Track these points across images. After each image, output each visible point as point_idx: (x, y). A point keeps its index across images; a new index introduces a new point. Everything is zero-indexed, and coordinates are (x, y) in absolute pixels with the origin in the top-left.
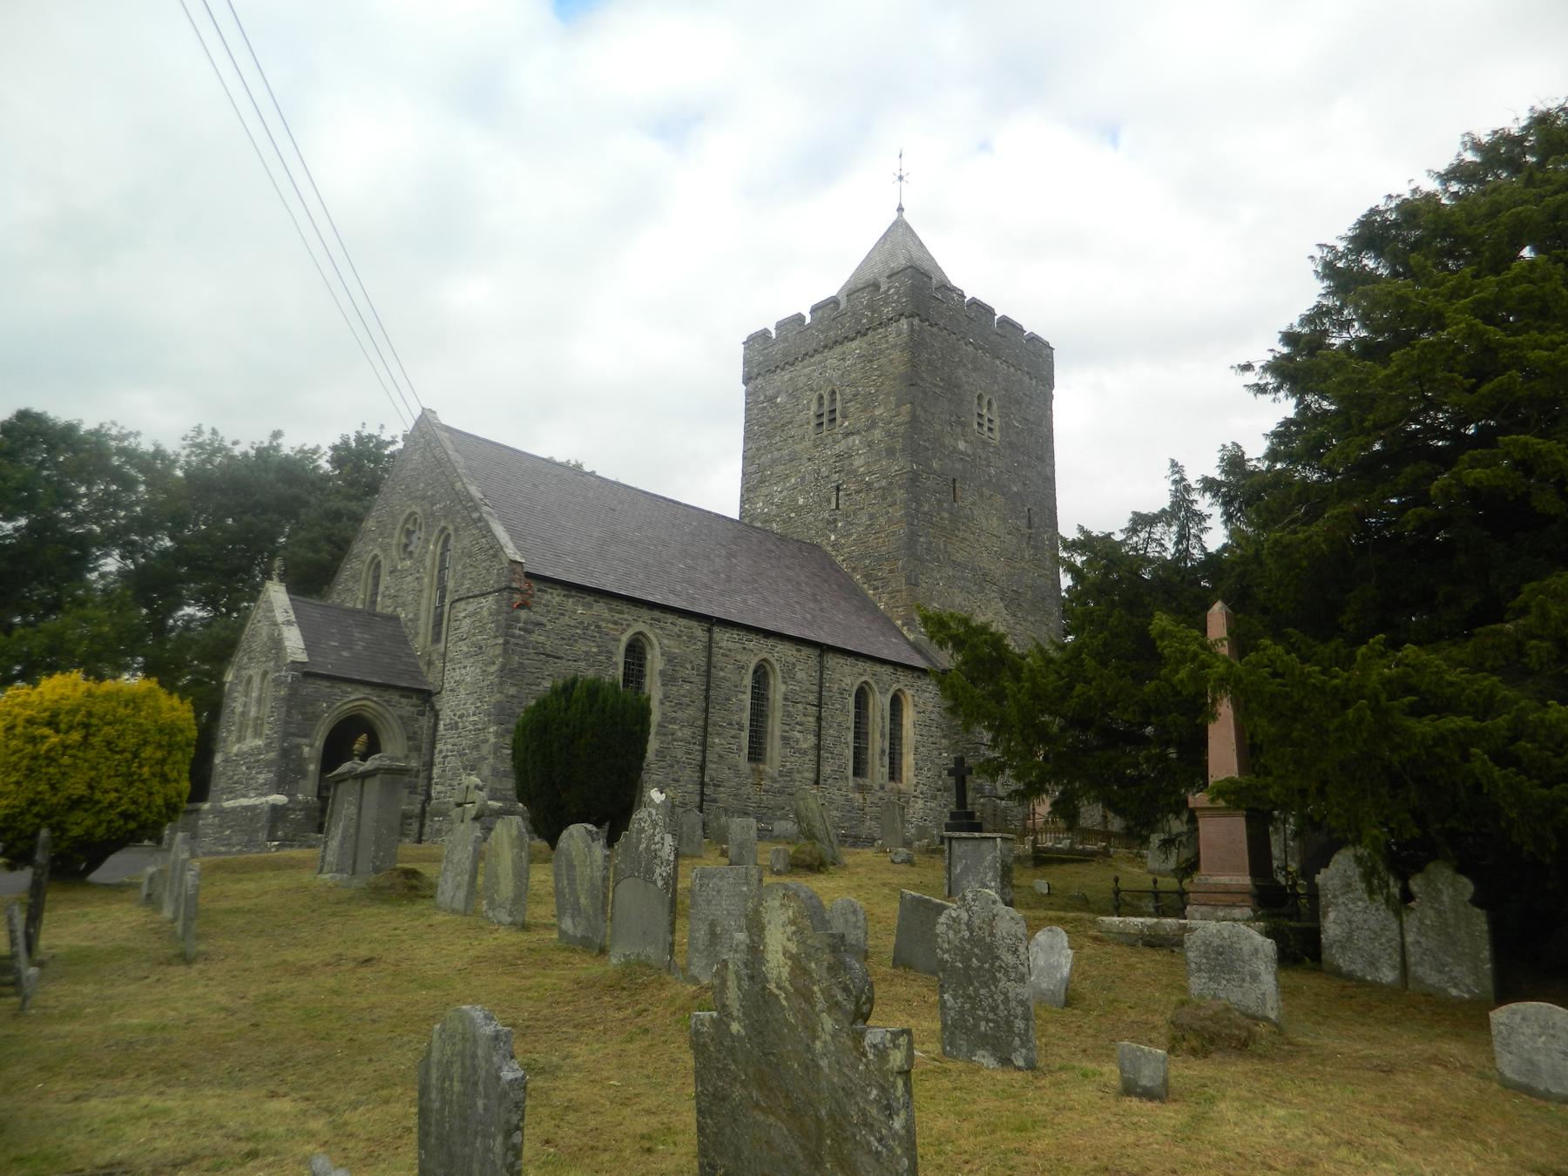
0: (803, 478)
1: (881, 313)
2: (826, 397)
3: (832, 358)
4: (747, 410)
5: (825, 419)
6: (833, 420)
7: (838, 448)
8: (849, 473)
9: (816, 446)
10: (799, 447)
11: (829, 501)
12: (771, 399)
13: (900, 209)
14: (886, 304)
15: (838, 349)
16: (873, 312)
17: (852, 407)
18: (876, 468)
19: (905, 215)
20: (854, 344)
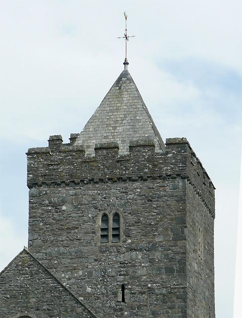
0: (90, 274)
1: (160, 168)
2: (111, 218)
3: (116, 189)
4: (31, 208)
5: (111, 233)
6: (116, 236)
7: (121, 258)
8: (132, 278)
9: (103, 252)
10: (85, 249)
11: (115, 294)
12: (56, 206)
13: (126, 63)
14: (166, 161)
15: (123, 185)
16: (155, 166)
17: (134, 231)
18: (158, 279)
19: (129, 68)
20: (136, 184)
